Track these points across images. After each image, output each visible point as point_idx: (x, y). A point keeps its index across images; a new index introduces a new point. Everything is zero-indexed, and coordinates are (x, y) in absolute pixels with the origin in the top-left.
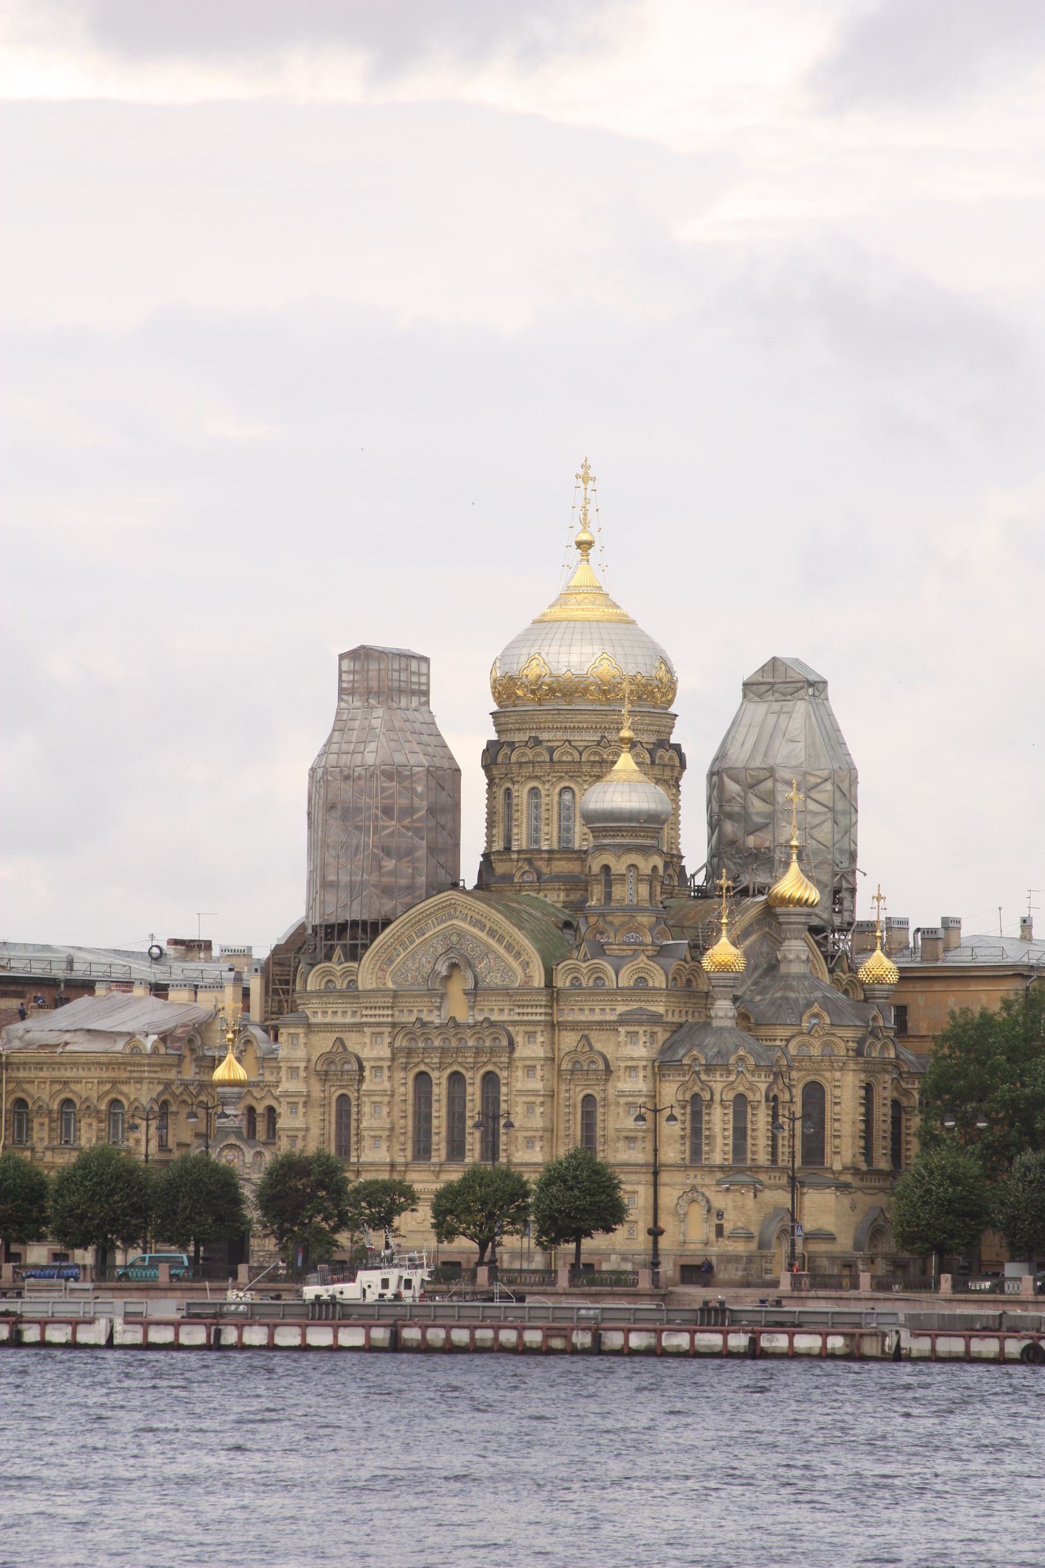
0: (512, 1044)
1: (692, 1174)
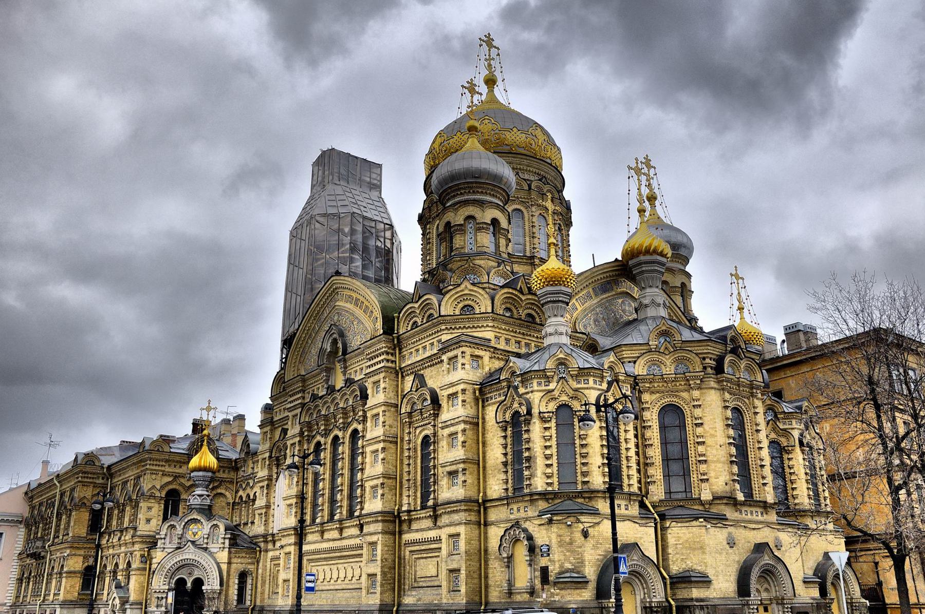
0: (364, 397)
1: (515, 507)
